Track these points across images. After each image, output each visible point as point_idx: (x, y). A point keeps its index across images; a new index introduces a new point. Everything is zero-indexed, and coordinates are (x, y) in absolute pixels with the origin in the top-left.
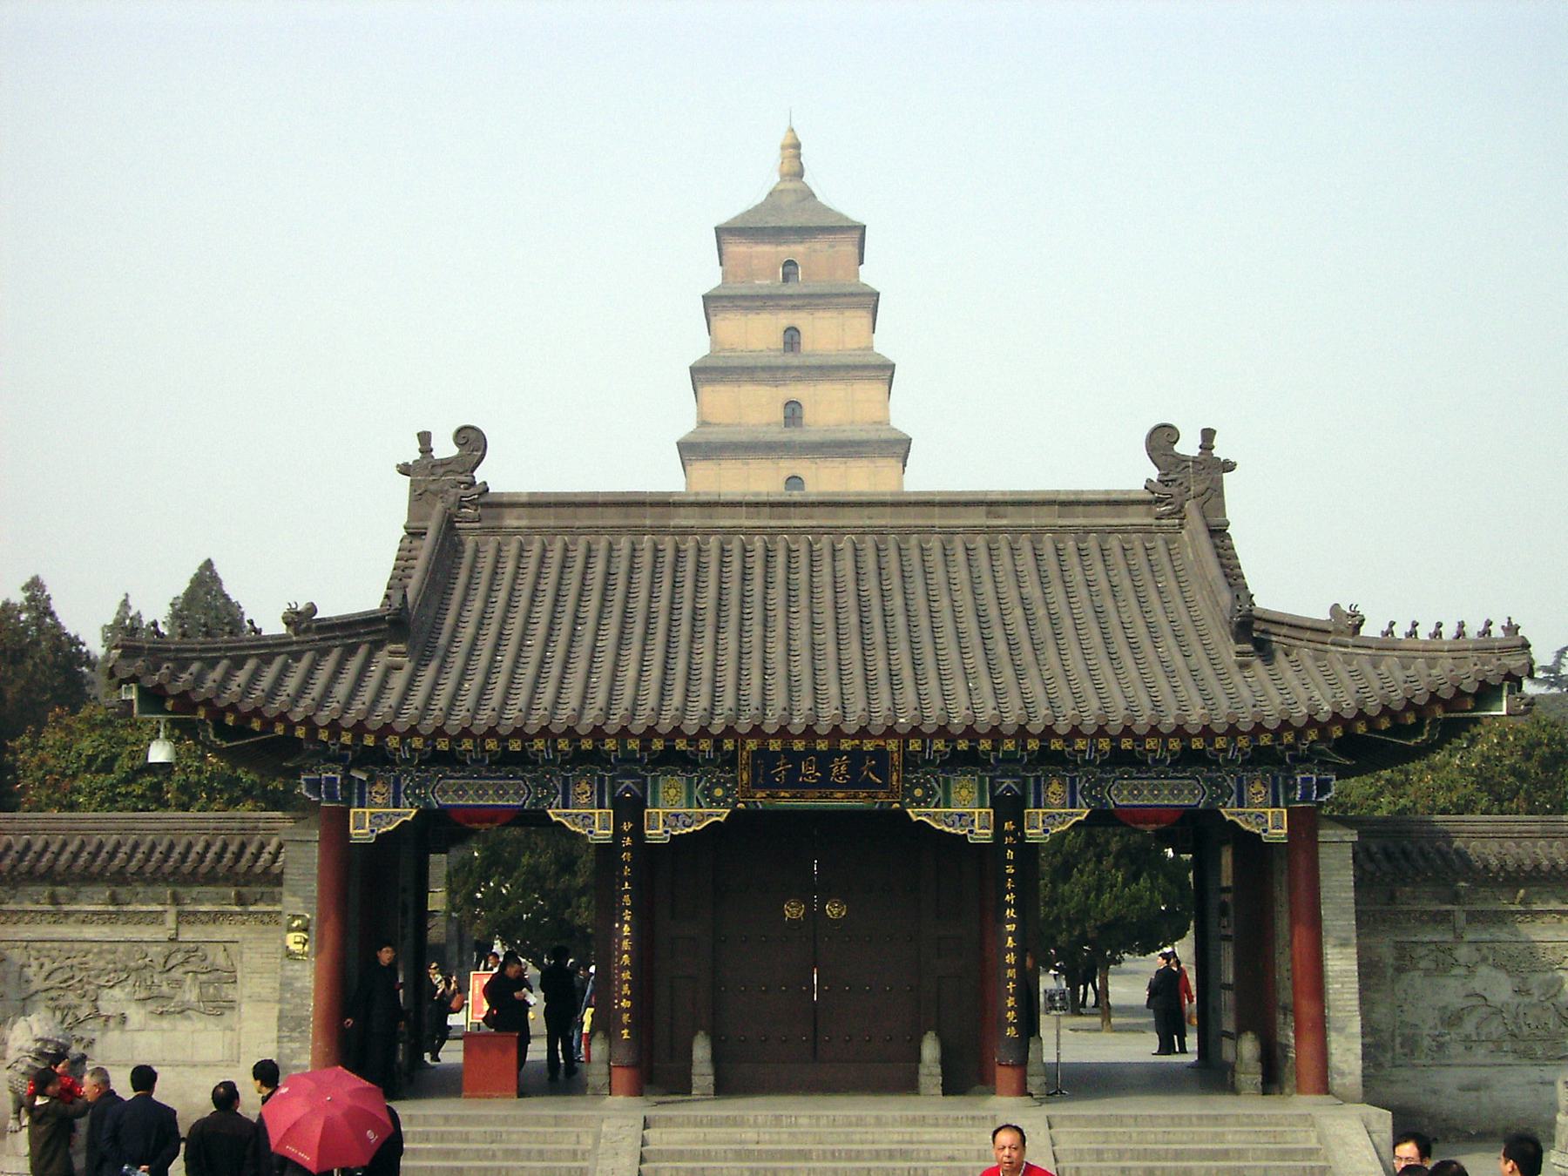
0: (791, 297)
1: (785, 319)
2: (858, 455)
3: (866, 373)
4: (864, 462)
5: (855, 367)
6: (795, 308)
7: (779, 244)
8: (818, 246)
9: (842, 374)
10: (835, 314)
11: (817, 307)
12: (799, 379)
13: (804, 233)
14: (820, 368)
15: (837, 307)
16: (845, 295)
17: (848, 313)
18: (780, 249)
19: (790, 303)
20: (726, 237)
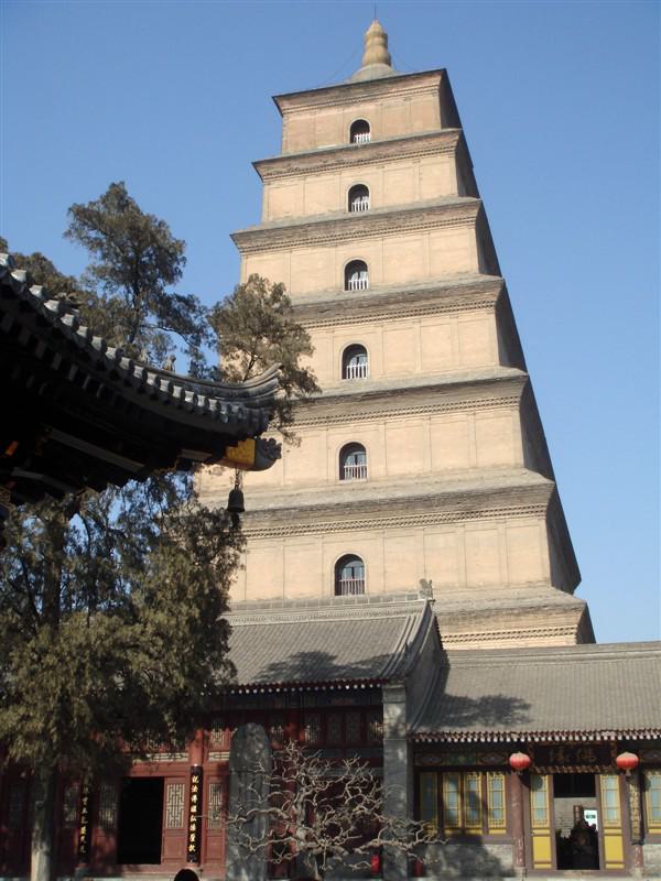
0: (356, 148)
1: (350, 178)
2: (435, 310)
3: (445, 217)
4: (444, 319)
5: (431, 210)
6: (360, 163)
7: (348, 105)
8: (392, 101)
9: (416, 221)
10: (409, 163)
11: (388, 158)
12: (364, 234)
13: (373, 86)
14: (388, 216)
15: (411, 155)
16: (419, 138)
17: (424, 161)
18: (346, 111)
19: (354, 157)
20: (286, 105)
